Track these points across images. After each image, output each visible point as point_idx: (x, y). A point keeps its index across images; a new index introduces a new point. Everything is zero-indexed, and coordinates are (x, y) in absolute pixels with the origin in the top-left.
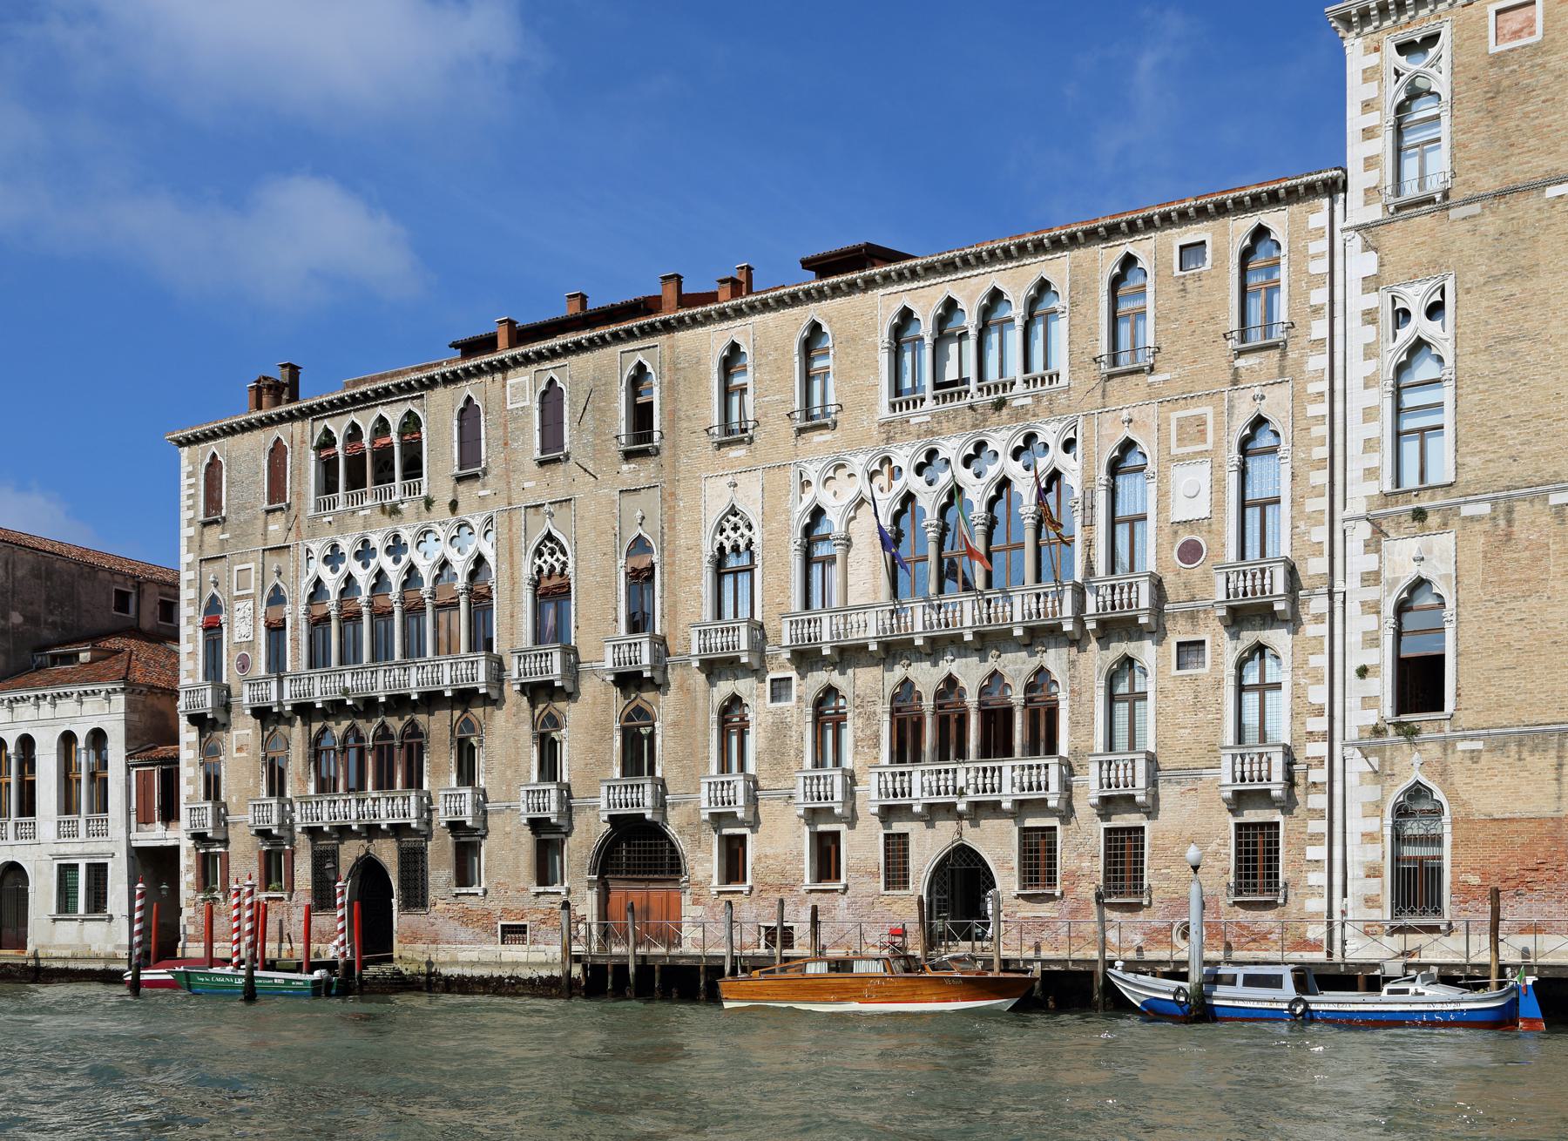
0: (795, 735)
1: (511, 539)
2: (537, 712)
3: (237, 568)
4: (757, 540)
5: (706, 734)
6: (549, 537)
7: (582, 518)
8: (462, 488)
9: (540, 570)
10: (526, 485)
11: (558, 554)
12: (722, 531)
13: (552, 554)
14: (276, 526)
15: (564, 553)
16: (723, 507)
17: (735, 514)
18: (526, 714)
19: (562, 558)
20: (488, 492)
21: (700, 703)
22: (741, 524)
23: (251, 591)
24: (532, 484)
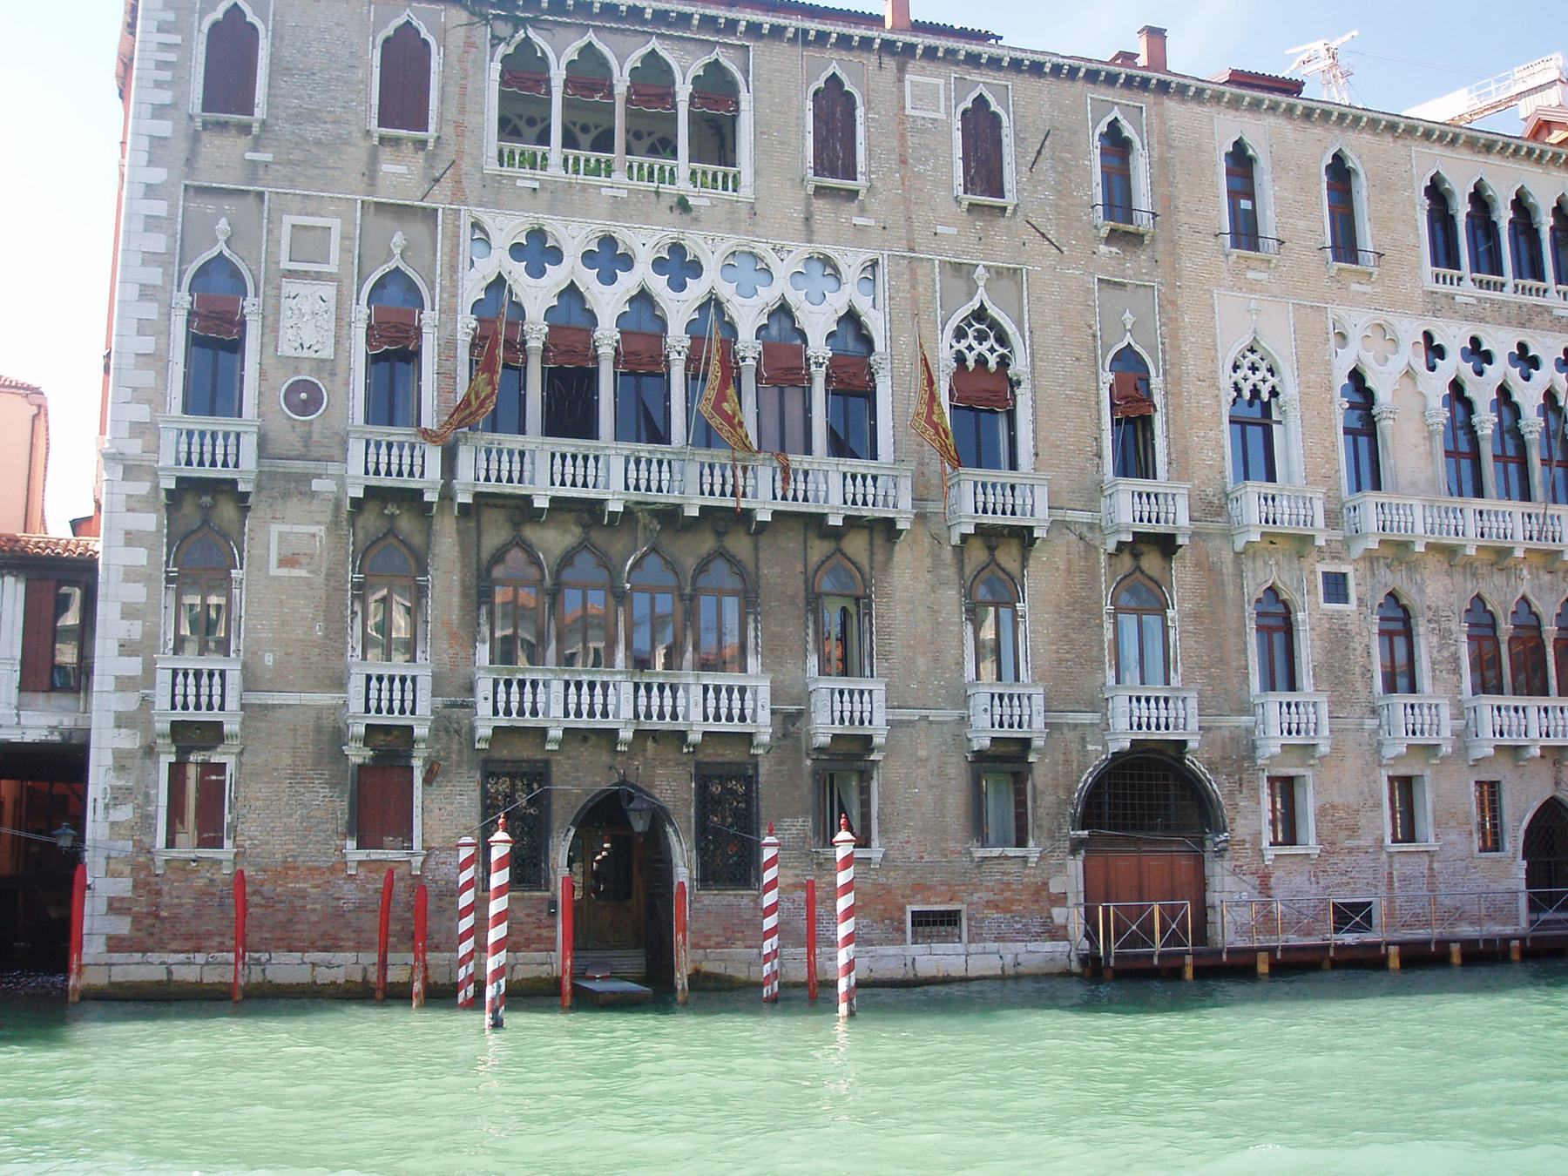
0: (1360, 649)
1: (915, 301)
2: (969, 570)
3: (289, 220)
4: (1290, 389)
5: (1242, 634)
6: (980, 314)
7: (1039, 299)
8: (819, 204)
9: (960, 359)
10: (940, 229)
11: (992, 341)
12: (1236, 367)
13: (981, 337)
14: (400, 174)
15: (1002, 339)
16: (1247, 341)
17: (1252, 351)
18: (950, 572)
19: (1001, 350)
20: (871, 222)
21: (1230, 591)
22: (1263, 366)
23: (332, 267)
24: (953, 231)
